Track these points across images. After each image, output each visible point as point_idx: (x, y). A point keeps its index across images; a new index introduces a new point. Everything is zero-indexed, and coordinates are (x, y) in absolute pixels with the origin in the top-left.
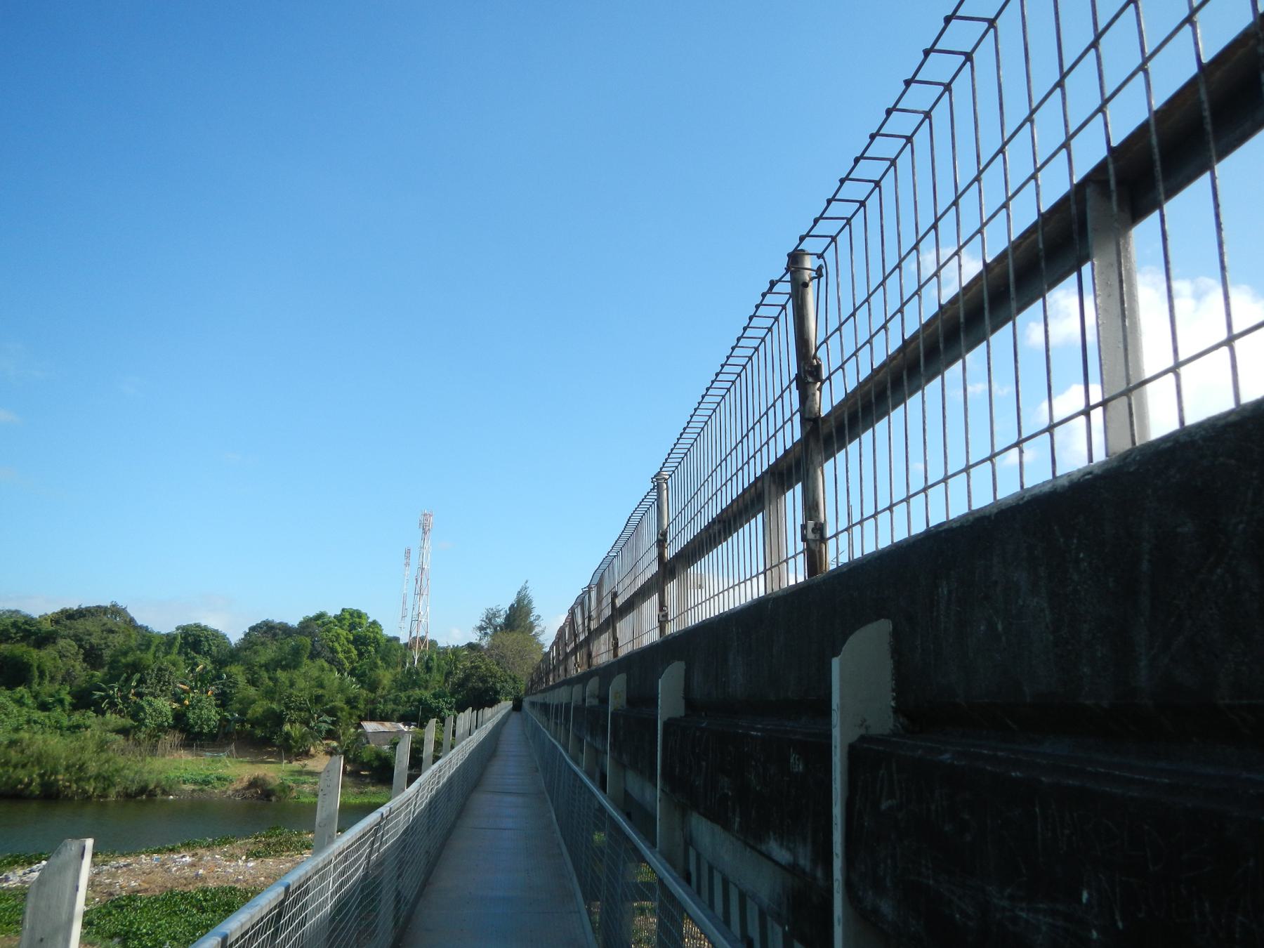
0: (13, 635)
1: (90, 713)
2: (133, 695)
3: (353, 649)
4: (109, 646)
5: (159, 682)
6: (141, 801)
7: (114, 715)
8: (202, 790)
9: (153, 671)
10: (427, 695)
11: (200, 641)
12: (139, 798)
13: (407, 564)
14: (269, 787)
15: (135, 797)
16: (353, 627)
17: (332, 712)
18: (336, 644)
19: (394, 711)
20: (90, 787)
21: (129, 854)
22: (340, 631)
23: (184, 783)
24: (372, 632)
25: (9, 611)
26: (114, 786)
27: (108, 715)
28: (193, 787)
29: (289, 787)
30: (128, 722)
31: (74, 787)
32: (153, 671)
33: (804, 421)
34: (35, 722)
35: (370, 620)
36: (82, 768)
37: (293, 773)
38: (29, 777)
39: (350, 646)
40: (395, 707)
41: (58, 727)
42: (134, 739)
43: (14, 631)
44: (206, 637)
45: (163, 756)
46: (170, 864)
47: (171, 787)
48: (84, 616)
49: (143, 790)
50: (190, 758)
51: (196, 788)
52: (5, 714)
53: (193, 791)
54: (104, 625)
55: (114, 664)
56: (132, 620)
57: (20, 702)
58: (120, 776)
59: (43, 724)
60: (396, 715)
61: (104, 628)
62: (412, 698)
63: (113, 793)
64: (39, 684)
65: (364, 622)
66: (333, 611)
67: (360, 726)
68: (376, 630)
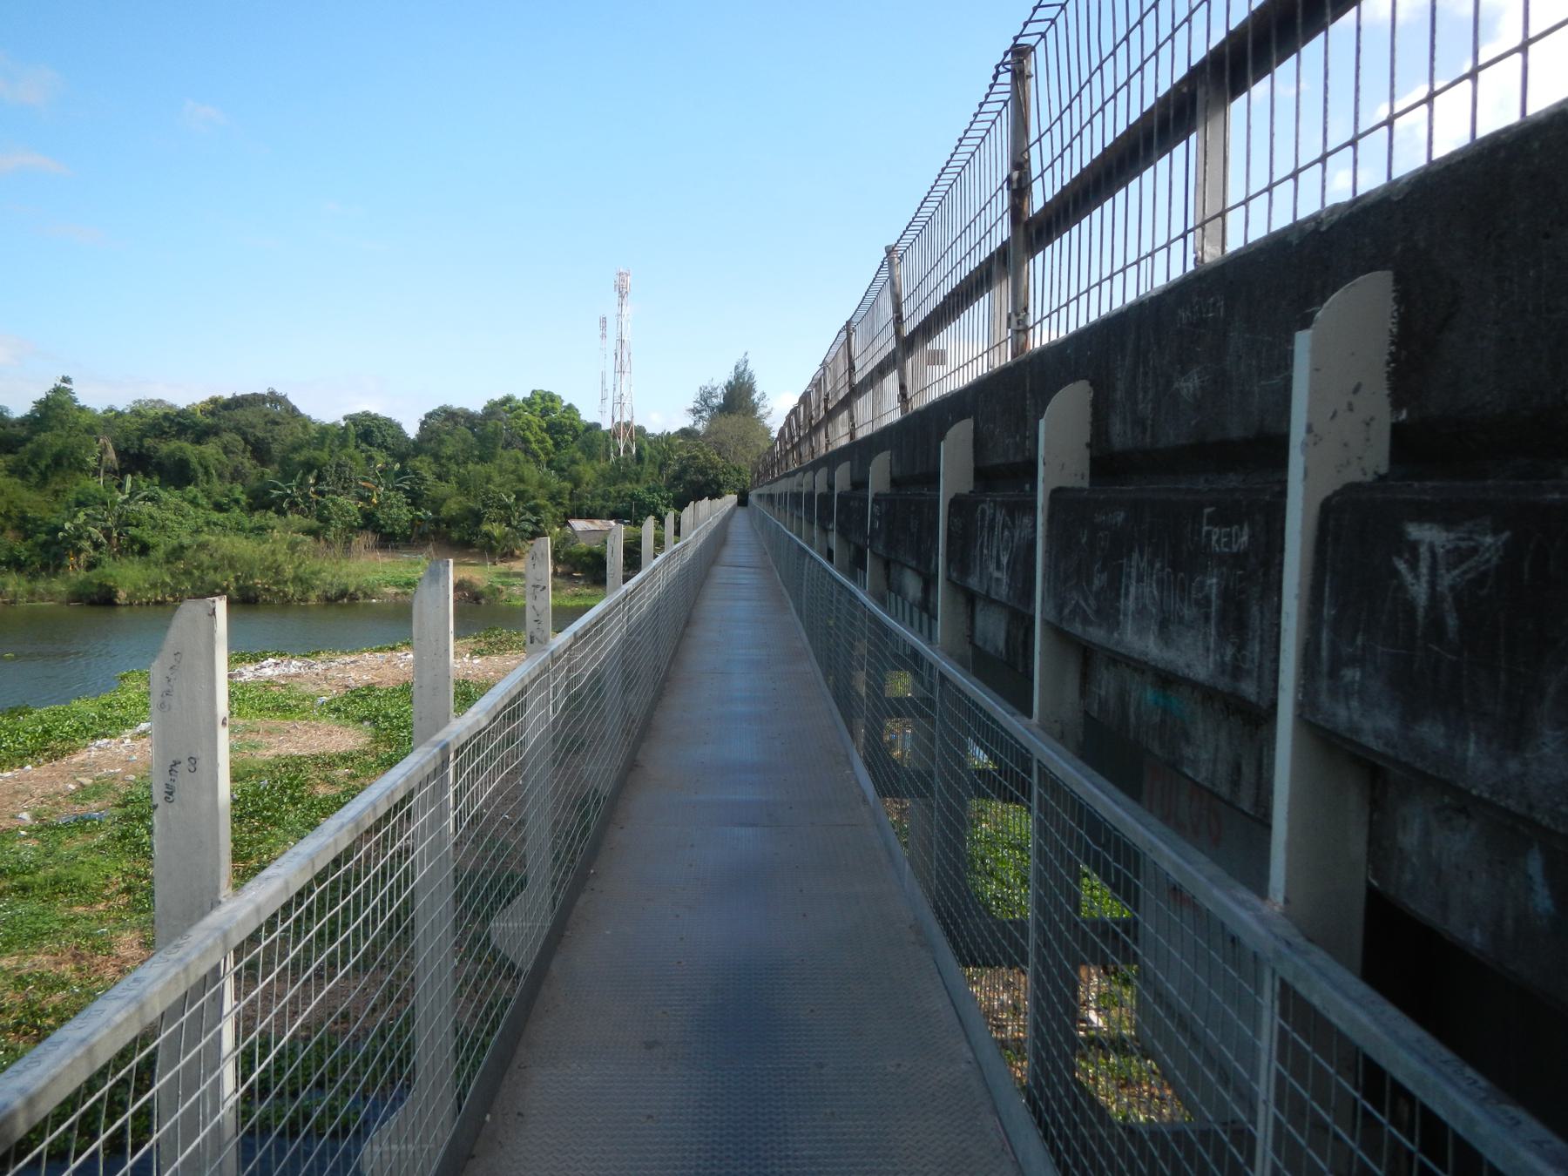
0: (167, 430)
1: (271, 514)
2: (313, 493)
3: (548, 439)
4: (276, 440)
5: (340, 479)
6: (342, 606)
7: (296, 516)
8: (406, 594)
9: (331, 467)
10: (640, 489)
11: (372, 431)
12: (340, 602)
13: (604, 336)
14: (477, 590)
15: (337, 599)
16: (545, 412)
17: (535, 510)
18: (528, 433)
19: (603, 507)
20: (290, 589)
21: (352, 652)
22: (530, 417)
23: (386, 587)
24: (568, 418)
25: (151, 401)
26: (313, 589)
27: (289, 516)
28: (395, 590)
29: (498, 589)
30: (315, 523)
32: (331, 467)
33: (850, 386)
34: (215, 524)
35: (565, 404)
36: (278, 570)
37: (499, 575)
39: (544, 435)
40: (605, 503)
41: (239, 529)
42: (326, 540)
43: (166, 424)
44: (378, 427)
45: (358, 558)
46: (395, 660)
47: (372, 590)
48: (242, 406)
49: (343, 594)
50: (386, 560)
51: (399, 591)
52: (182, 516)
53: (396, 594)
54: (266, 415)
55: (285, 462)
56: (294, 409)
57: (194, 502)
58: (317, 579)
59: (224, 526)
60: (606, 512)
61: (266, 419)
62: (623, 493)
63: (313, 597)
64: (208, 483)
65: (557, 405)
66: (521, 393)
67: (567, 523)
68: (572, 415)
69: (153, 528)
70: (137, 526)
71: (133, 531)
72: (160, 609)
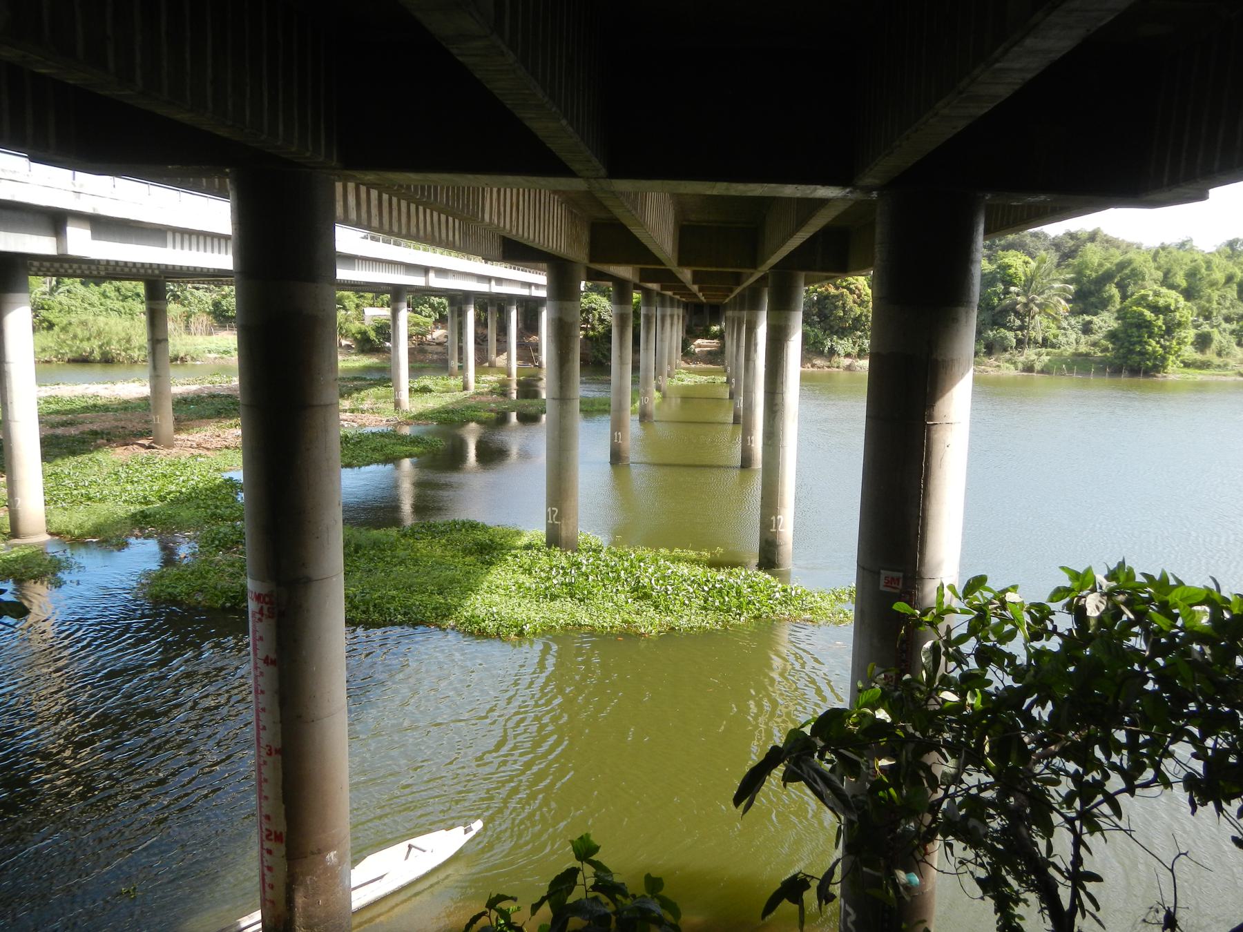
8: (222, 358)
20: (135, 354)
38: (92, 347)
51: (218, 356)
53: (216, 358)
59: (119, 312)
69: (60, 311)
71: (44, 313)
72: (47, 365)
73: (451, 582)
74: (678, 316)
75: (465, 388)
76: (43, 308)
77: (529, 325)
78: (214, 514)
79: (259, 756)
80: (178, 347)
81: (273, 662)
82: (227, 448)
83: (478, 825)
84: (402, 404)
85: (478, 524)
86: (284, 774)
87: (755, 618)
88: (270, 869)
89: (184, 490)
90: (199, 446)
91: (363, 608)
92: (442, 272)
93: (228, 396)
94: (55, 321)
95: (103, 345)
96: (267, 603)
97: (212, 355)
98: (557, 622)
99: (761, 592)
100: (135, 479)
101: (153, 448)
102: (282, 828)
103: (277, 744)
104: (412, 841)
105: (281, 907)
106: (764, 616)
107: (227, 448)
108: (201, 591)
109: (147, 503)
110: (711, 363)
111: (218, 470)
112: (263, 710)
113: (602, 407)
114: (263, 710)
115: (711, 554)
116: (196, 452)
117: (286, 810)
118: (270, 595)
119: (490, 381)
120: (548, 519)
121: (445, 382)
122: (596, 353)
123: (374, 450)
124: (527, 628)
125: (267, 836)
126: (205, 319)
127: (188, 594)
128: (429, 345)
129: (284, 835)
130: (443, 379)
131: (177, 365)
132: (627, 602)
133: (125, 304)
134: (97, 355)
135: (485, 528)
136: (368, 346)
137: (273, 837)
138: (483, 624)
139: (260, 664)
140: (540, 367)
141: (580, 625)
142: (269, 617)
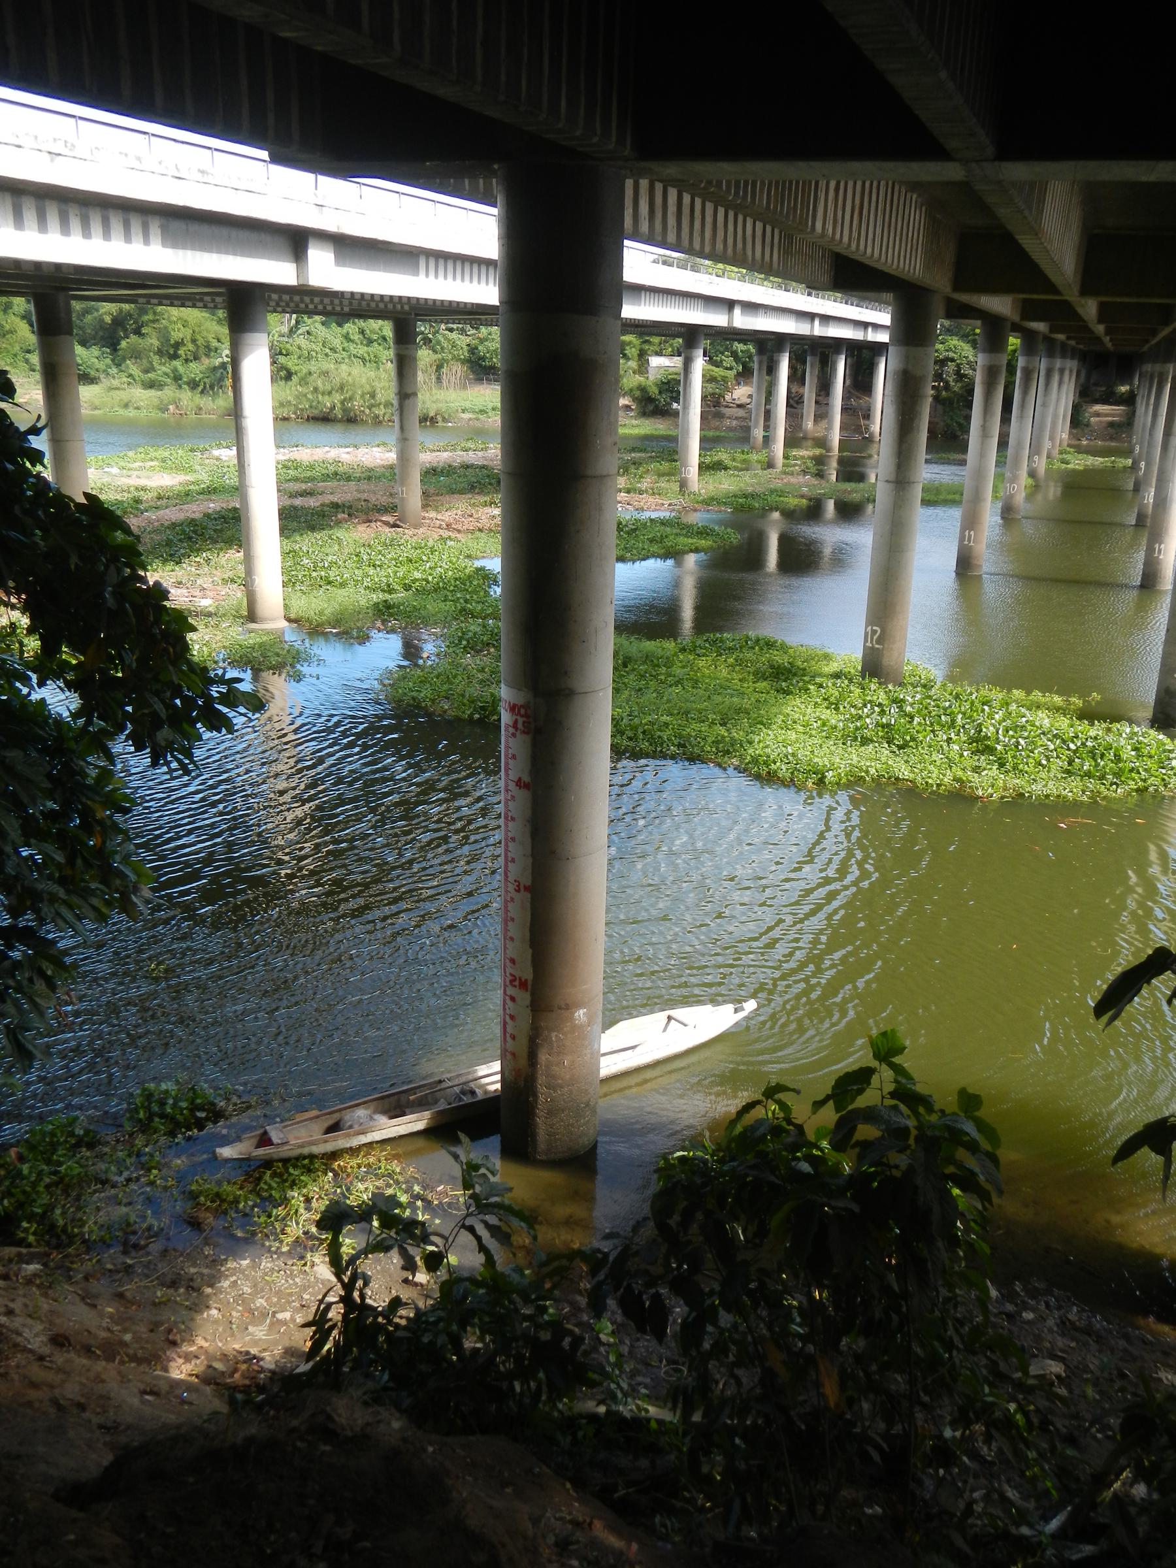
8: (477, 419)
20: (379, 412)
31: (367, 411)
53: (470, 419)
59: (363, 360)
70: (286, 355)
71: (282, 359)
73: (739, 711)
74: (1071, 371)
75: (770, 465)
76: (281, 353)
77: (861, 382)
78: (463, 609)
79: (506, 891)
80: (428, 404)
81: (526, 786)
82: (480, 530)
83: (751, 1005)
84: (690, 484)
85: (776, 642)
86: (532, 915)
87: (1137, 790)
88: (512, 1017)
89: (430, 578)
90: (448, 525)
91: (630, 734)
92: (751, 307)
93: (483, 467)
94: (293, 369)
95: (345, 399)
96: (522, 716)
97: (466, 416)
98: (867, 772)
99: (1151, 757)
100: (378, 563)
101: (398, 526)
102: (528, 974)
103: (527, 881)
104: (674, 1013)
105: (523, 1062)
106: (1151, 789)
107: (480, 530)
108: (448, 698)
109: (390, 591)
110: (1112, 439)
111: (469, 557)
112: (513, 839)
113: (950, 497)
114: (513, 839)
115: (1084, 701)
116: (446, 534)
117: (533, 955)
118: (525, 706)
119: (803, 457)
120: (866, 641)
121: (745, 457)
122: (949, 421)
123: (651, 541)
124: (829, 775)
125: (511, 981)
126: (458, 369)
127: (433, 701)
128: (727, 407)
129: (530, 983)
130: (743, 452)
131: (426, 426)
132: (961, 756)
133: (370, 349)
134: (338, 413)
135: (784, 648)
136: (651, 407)
137: (517, 983)
138: (773, 767)
139: (512, 786)
140: (870, 440)
141: (897, 779)
142: (524, 732)
